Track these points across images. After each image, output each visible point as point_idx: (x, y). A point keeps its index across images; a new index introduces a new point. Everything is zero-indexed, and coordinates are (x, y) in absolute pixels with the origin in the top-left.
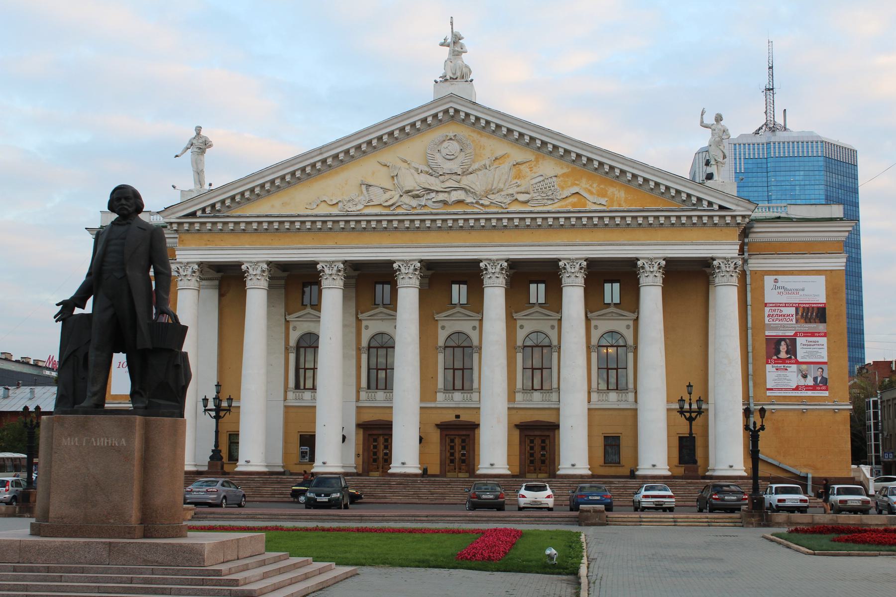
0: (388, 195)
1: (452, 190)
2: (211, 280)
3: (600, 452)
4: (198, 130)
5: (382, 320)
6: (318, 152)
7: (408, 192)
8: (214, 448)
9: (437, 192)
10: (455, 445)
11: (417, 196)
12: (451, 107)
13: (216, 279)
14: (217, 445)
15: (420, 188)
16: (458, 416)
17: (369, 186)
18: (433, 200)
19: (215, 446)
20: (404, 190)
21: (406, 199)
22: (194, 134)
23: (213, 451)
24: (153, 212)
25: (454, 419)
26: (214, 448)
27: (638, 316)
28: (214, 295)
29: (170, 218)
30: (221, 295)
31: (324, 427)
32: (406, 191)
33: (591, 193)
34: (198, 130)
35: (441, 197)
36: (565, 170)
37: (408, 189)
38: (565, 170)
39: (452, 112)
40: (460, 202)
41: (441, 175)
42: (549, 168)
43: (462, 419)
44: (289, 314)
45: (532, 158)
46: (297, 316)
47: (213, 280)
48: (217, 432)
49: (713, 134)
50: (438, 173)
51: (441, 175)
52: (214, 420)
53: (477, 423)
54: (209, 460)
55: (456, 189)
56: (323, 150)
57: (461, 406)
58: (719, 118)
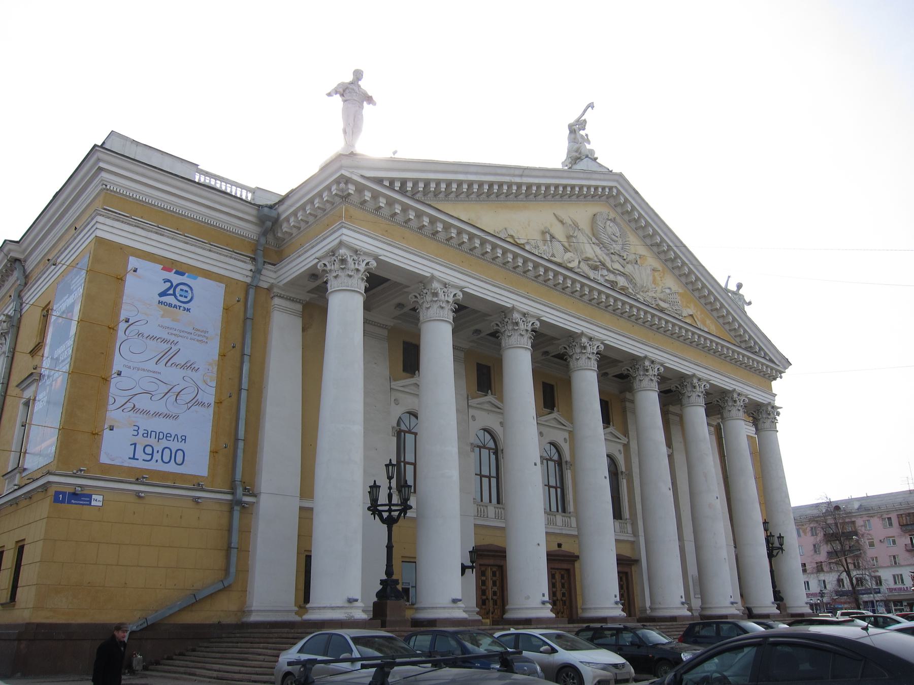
0: (569, 255)
1: (618, 274)
2: (293, 300)
3: (552, 595)
4: (358, 75)
5: (489, 411)
6: (521, 173)
7: (587, 259)
8: (385, 577)
9: (608, 270)
10: (556, 582)
11: (595, 268)
12: (616, 187)
13: (299, 302)
14: (389, 571)
15: (598, 260)
16: (560, 545)
17: (552, 237)
18: (607, 278)
19: (386, 573)
20: (584, 256)
21: (585, 268)
22: (349, 78)
23: (382, 582)
24: (202, 170)
25: (556, 548)
26: (385, 577)
27: (673, 452)
28: (298, 323)
29: (352, 173)
30: (304, 330)
31: (539, 547)
32: (586, 257)
33: (698, 320)
34: (358, 75)
35: (611, 277)
36: (681, 291)
37: (589, 255)
38: (681, 291)
39: (615, 191)
40: (623, 288)
41: (612, 253)
42: (670, 283)
43: (564, 548)
44: (395, 380)
45: (660, 268)
46: (402, 384)
47: (296, 301)
48: (390, 547)
49: (744, 300)
50: (608, 250)
51: (612, 253)
52: (386, 526)
53: (576, 554)
54: (376, 599)
55: (623, 274)
56: (526, 173)
57: (564, 532)
58: (740, 286)
